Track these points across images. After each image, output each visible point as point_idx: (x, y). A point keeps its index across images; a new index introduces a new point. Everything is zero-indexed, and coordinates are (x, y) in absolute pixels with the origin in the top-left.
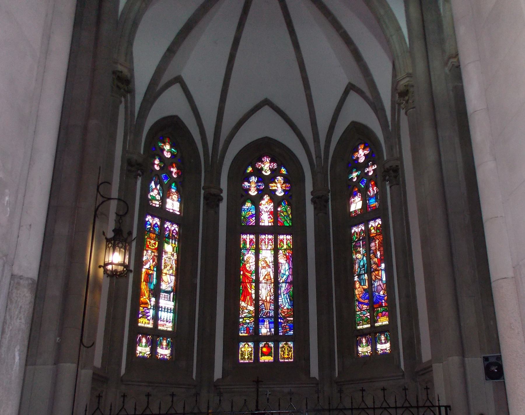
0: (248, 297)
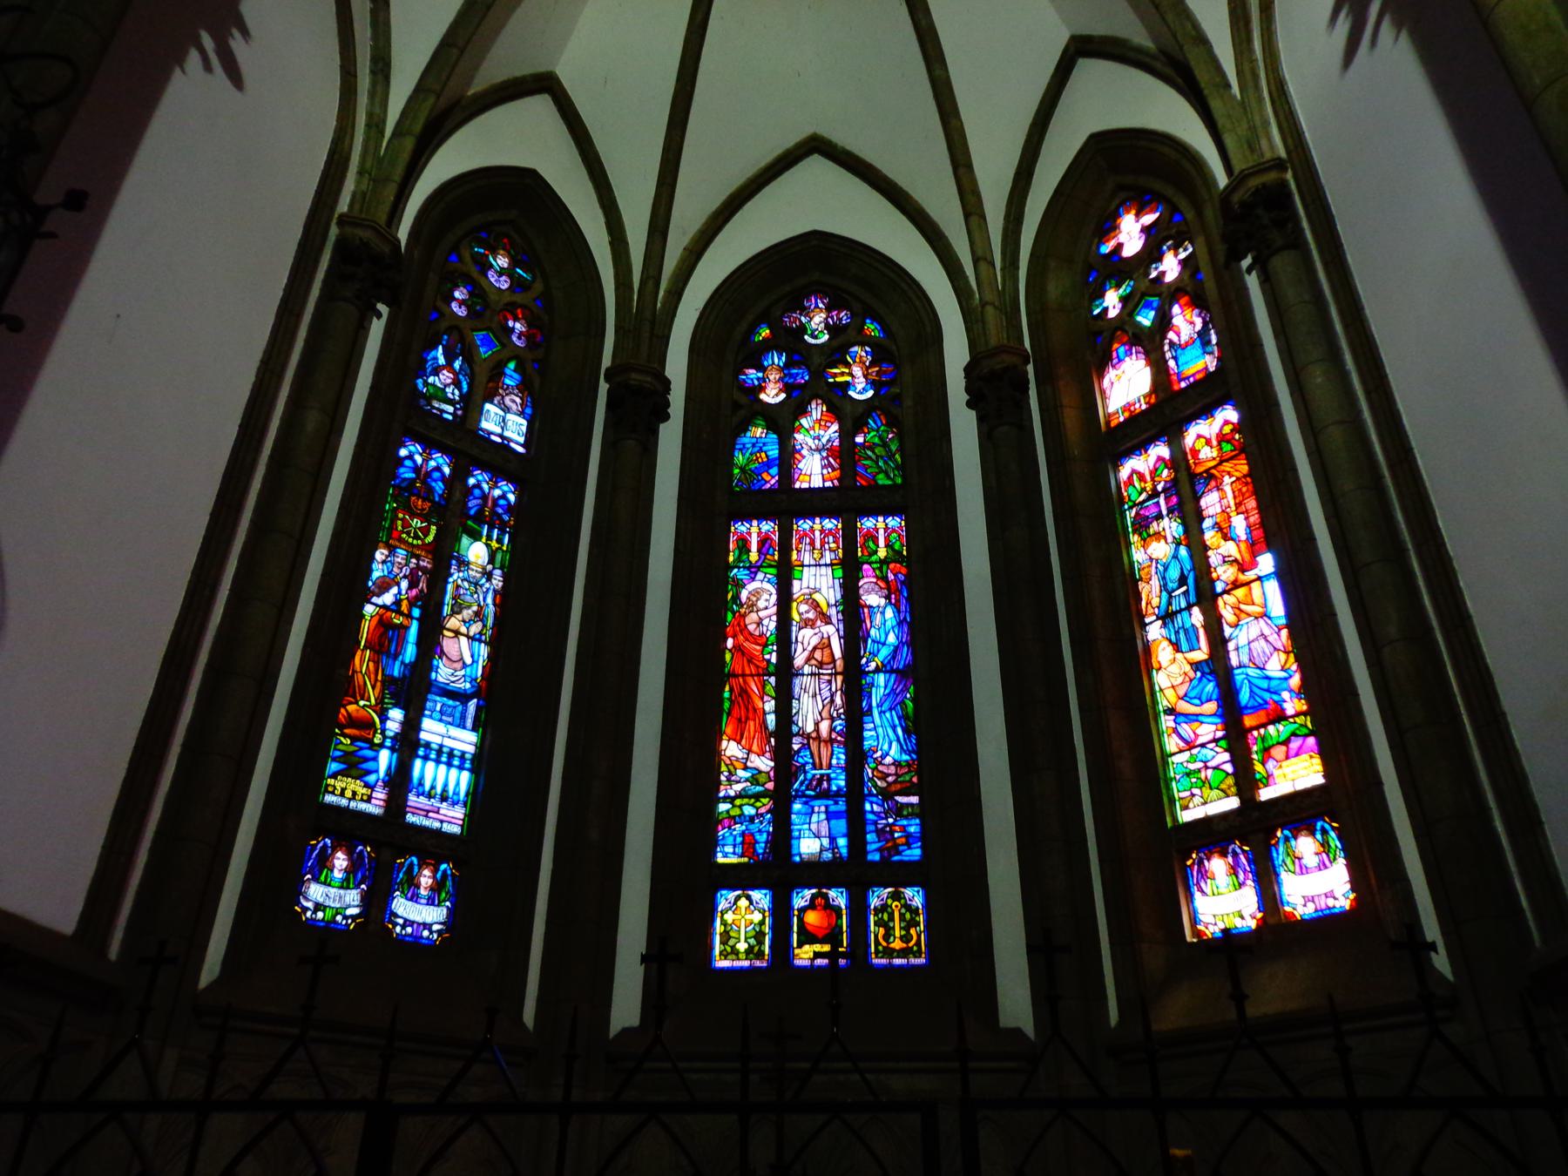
0: (752, 723)
